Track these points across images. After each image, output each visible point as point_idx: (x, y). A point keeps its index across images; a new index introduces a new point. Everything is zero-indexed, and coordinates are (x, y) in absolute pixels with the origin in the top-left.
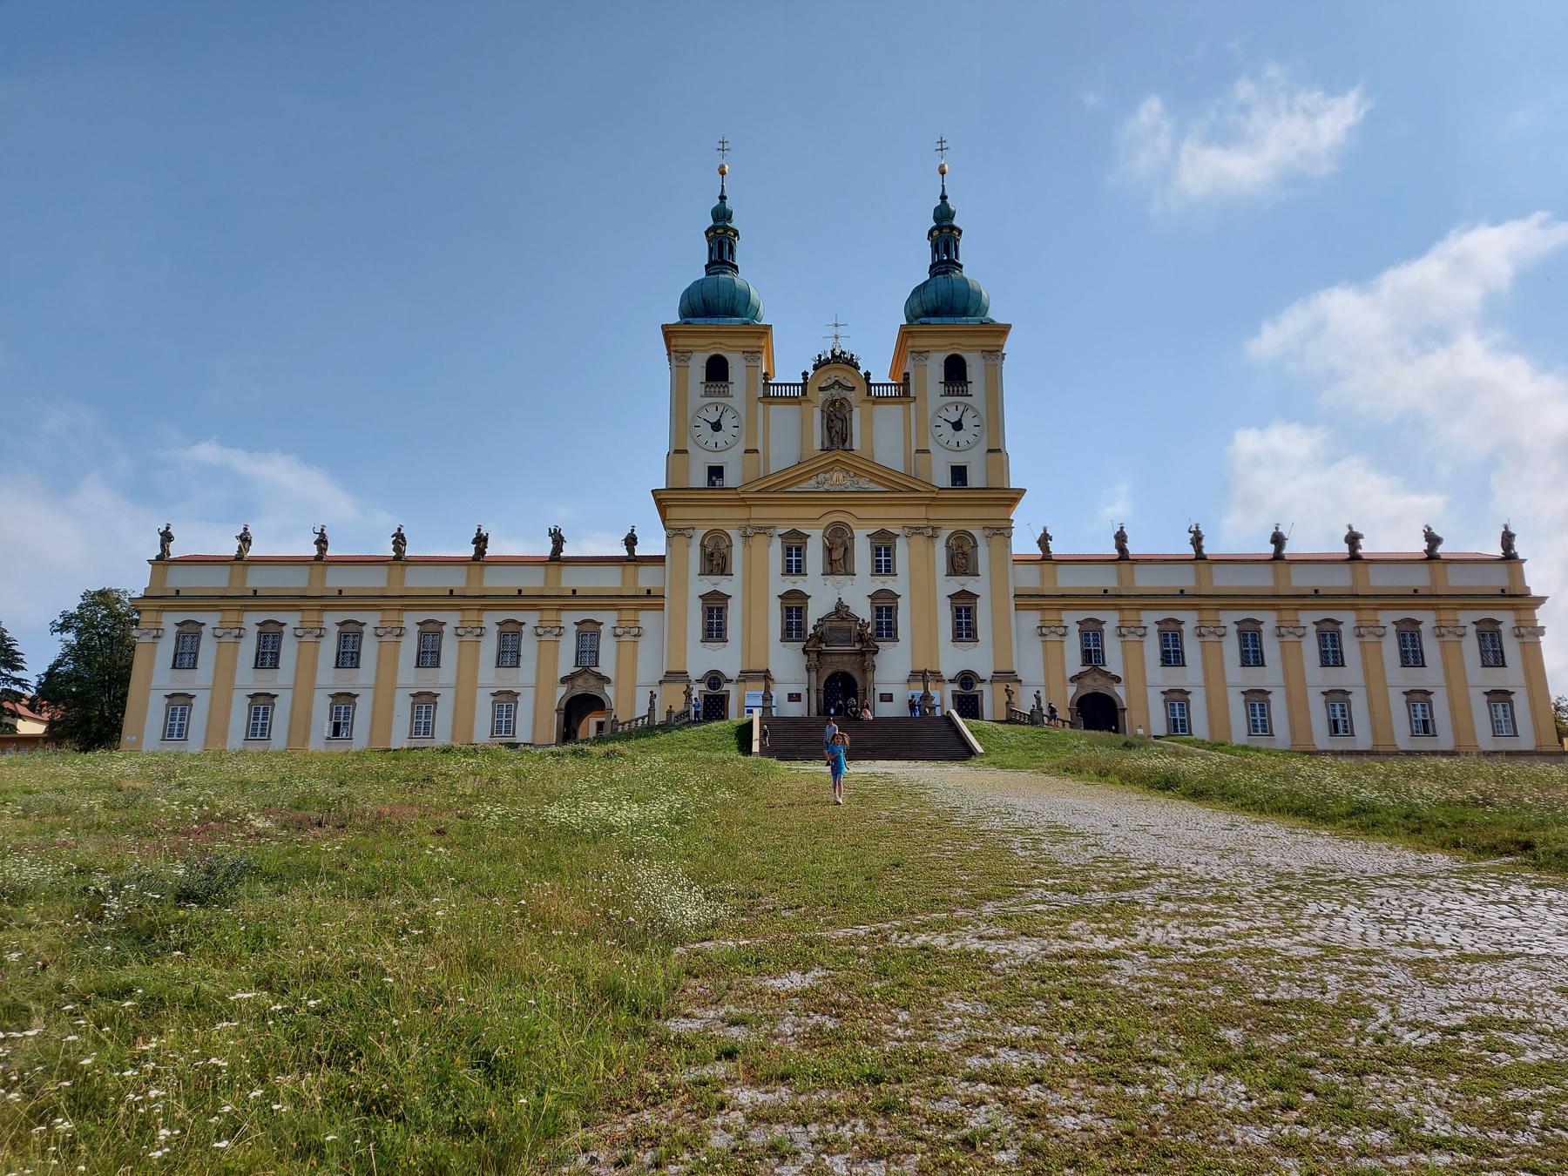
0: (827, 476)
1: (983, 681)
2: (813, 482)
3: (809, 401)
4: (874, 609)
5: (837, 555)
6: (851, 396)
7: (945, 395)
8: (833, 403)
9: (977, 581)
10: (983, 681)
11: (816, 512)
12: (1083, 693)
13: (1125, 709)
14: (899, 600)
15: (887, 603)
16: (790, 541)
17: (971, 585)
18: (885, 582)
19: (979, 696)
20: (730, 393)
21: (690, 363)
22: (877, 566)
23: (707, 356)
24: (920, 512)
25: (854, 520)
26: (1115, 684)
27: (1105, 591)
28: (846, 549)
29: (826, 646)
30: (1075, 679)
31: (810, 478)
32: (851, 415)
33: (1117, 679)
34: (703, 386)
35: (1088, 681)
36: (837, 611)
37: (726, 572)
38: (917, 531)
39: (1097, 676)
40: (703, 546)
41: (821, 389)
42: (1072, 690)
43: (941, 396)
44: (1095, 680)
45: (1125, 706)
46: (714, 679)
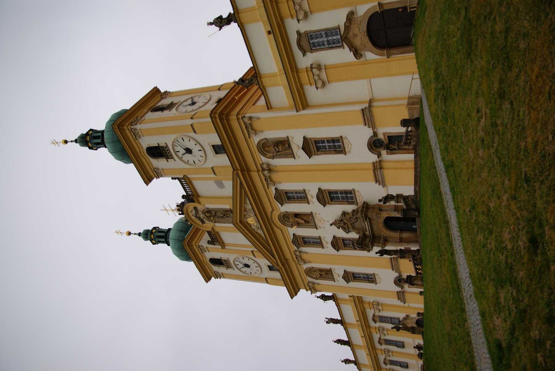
1: (375, 134)
2: (260, 232)
9: (293, 138)
10: (375, 134)
11: (278, 232)
12: (370, 45)
13: (379, 3)
17: (297, 142)
19: (388, 135)
24: (255, 175)
25: (275, 212)
26: (355, 16)
27: (269, 33)
29: (366, 231)
30: (357, 54)
31: (257, 233)
33: (350, 17)
35: (357, 42)
38: (269, 181)
39: (351, 34)
41: (203, 222)
42: (370, 55)
44: (355, 36)
45: (377, 3)
46: (399, 281)
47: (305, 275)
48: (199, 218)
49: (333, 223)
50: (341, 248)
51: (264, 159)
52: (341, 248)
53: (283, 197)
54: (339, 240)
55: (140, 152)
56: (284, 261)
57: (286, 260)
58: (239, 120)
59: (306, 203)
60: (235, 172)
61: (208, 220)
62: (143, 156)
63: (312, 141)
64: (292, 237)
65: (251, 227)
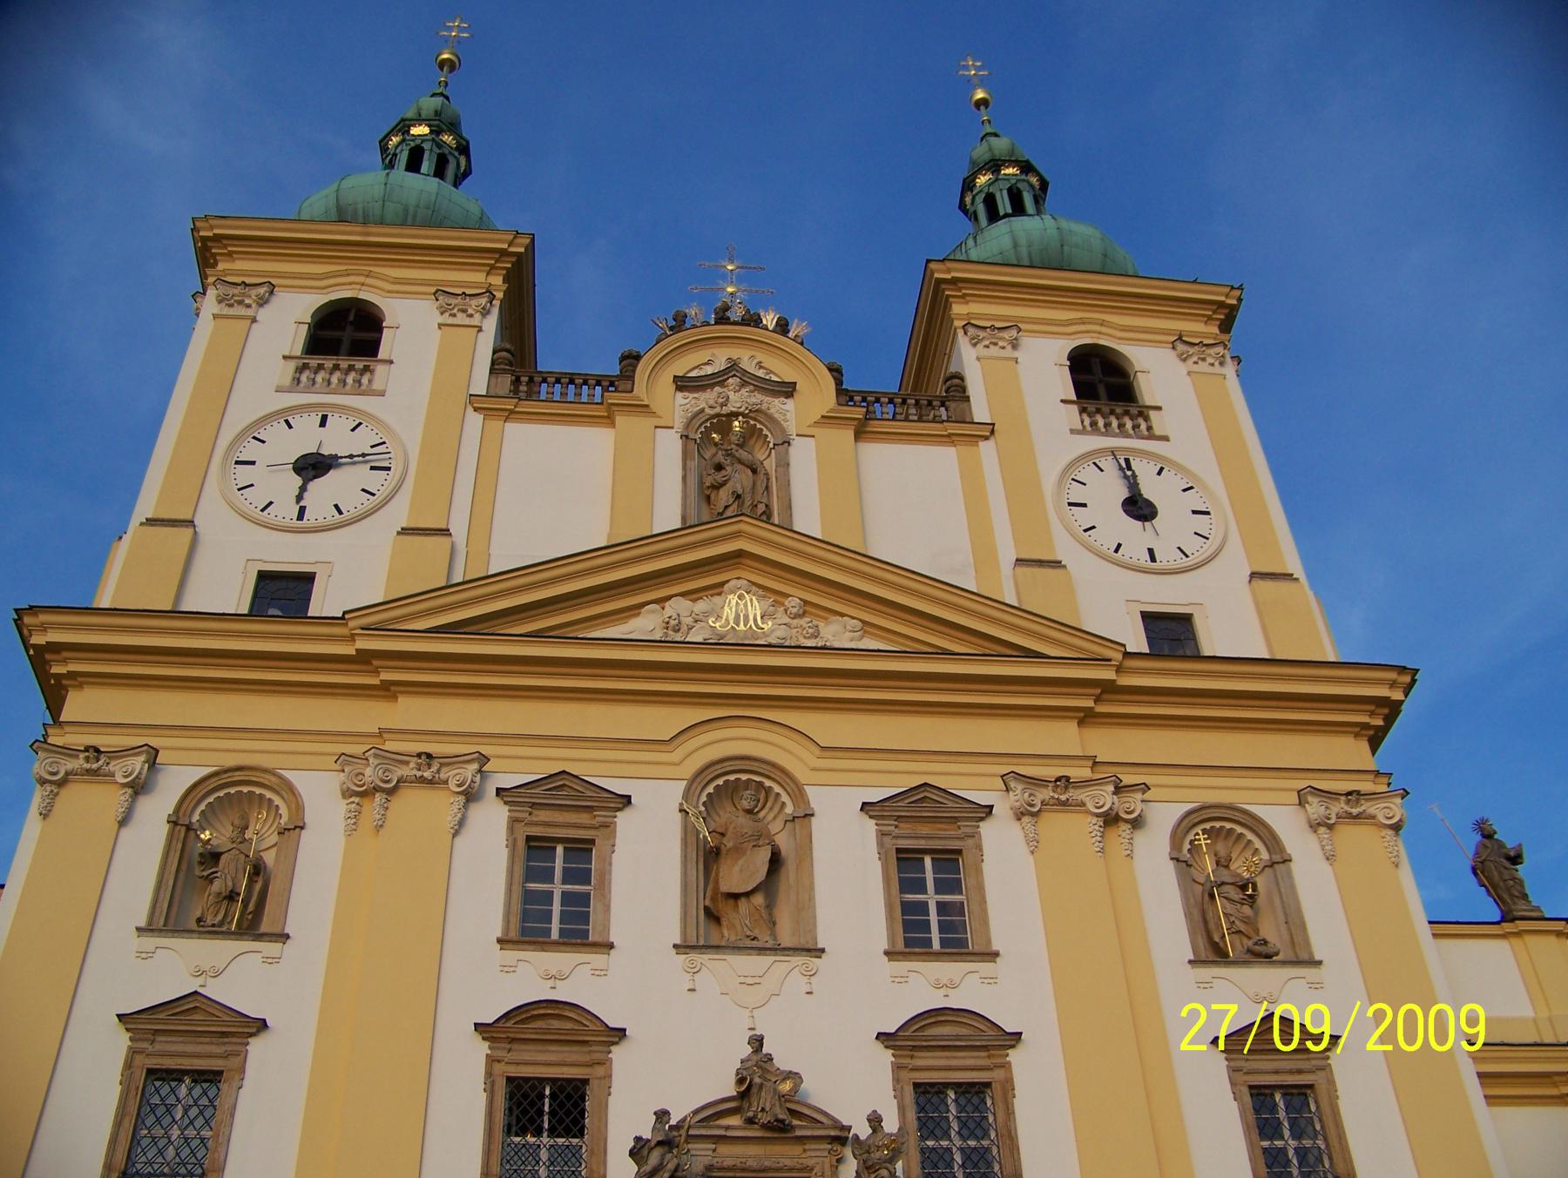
0: (701, 606)
2: (646, 624)
3: (643, 409)
4: (909, 1090)
5: (742, 873)
6: (787, 411)
7: (1083, 431)
8: (722, 422)
11: (663, 721)
14: (1014, 1056)
15: (962, 1068)
16: (544, 815)
18: (953, 986)
20: (376, 386)
21: (263, 314)
22: (908, 926)
23: (317, 300)
24: (1063, 737)
25: (810, 757)
28: (776, 861)
32: (784, 465)
34: (291, 366)
36: (746, 1089)
37: (264, 928)
40: (180, 824)
41: (683, 384)
43: (1072, 431)
47: (231, 761)
48: (717, 379)
49: (770, 1058)
50: (499, 1054)
51: (1164, 815)
52: (499, 1054)
53: (925, 829)
54: (586, 1058)
55: (1102, 323)
56: (386, 676)
57: (388, 691)
58: (1371, 777)
59: (892, 938)
60: (1119, 656)
61: (702, 410)
62: (1082, 322)
63: (1310, 1072)
64: (619, 787)
65: (682, 595)
